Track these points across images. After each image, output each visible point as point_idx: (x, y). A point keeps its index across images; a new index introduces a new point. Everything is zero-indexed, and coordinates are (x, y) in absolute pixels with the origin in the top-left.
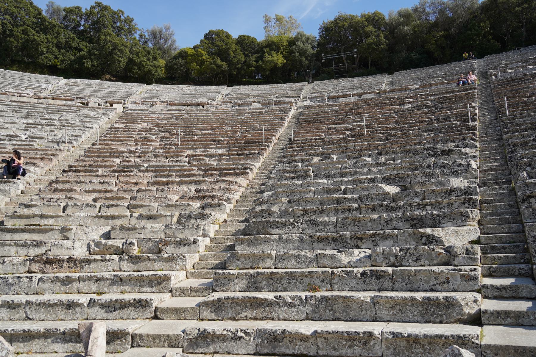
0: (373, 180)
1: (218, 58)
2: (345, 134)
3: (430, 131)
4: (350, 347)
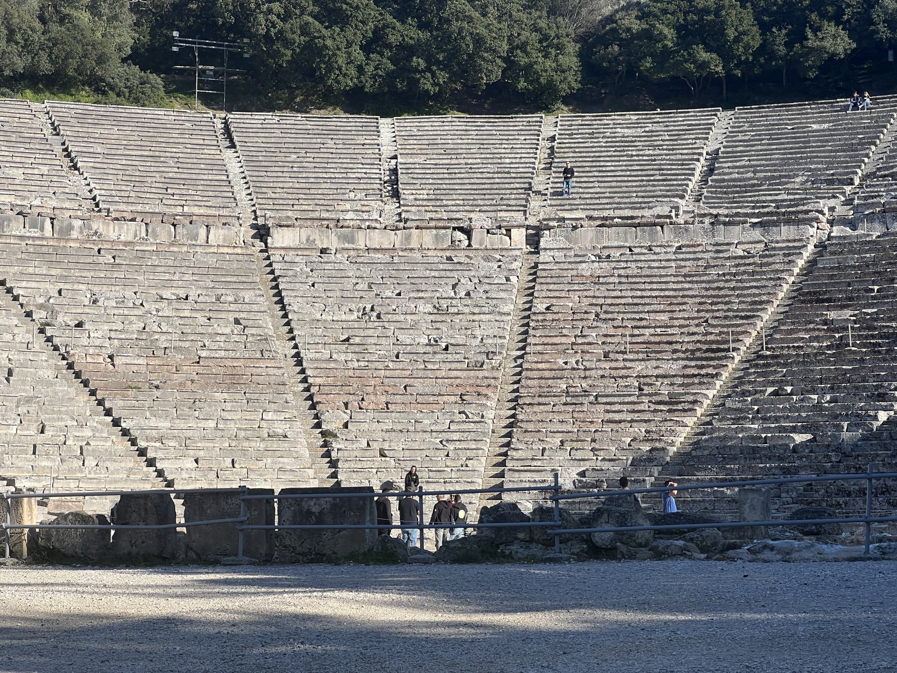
1: (701, 46)
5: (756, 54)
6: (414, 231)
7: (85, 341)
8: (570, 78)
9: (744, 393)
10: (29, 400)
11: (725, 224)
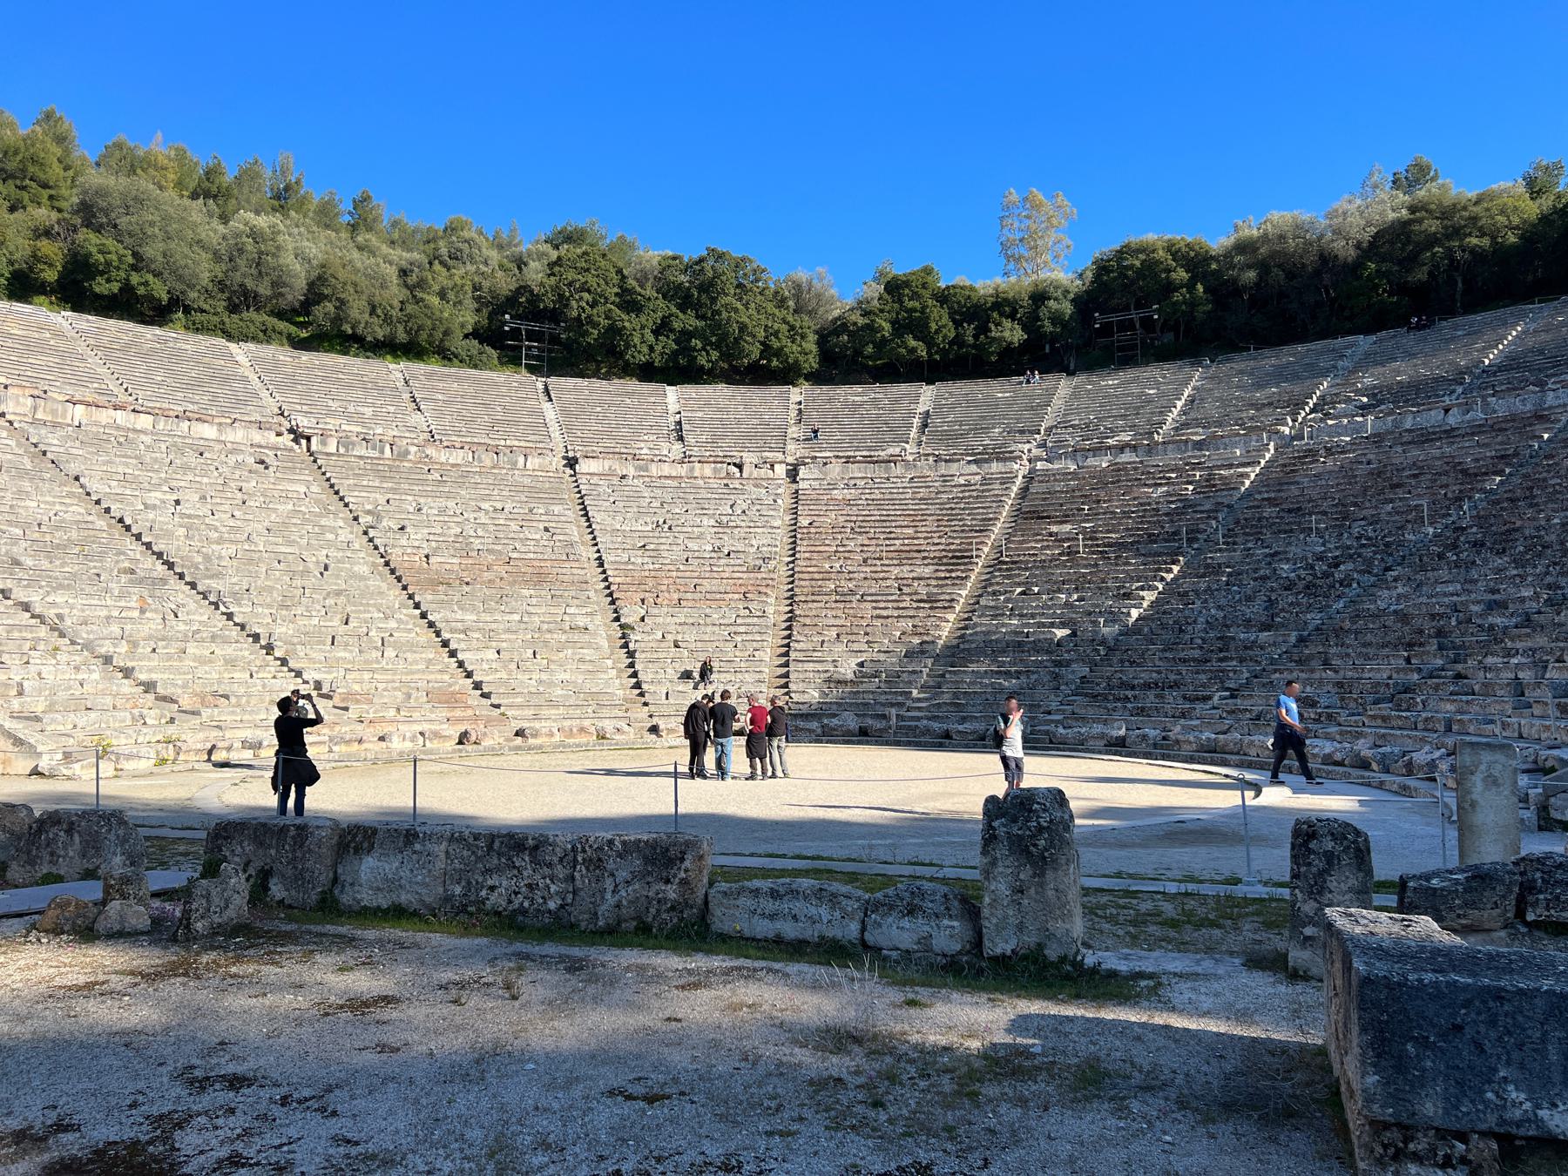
5: (951, 343)
6: (697, 464)
7: (404, 542)
8: (811, 360)
9: (994, 593)
10: (338, 593)
11: (946, 461)
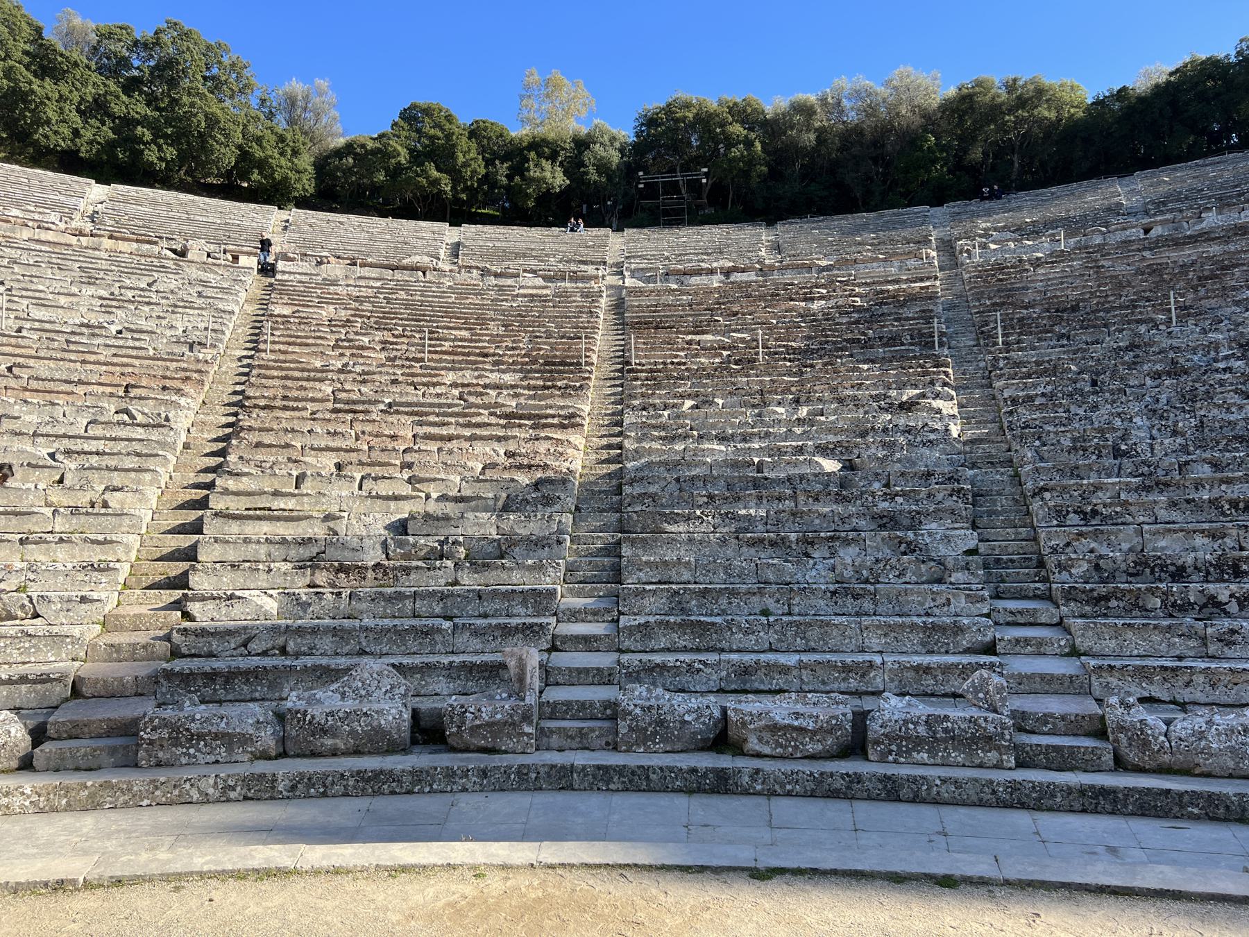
0: (800, 450)
2: (721, 355)
3: (873, 362)
4: (844, 680)
